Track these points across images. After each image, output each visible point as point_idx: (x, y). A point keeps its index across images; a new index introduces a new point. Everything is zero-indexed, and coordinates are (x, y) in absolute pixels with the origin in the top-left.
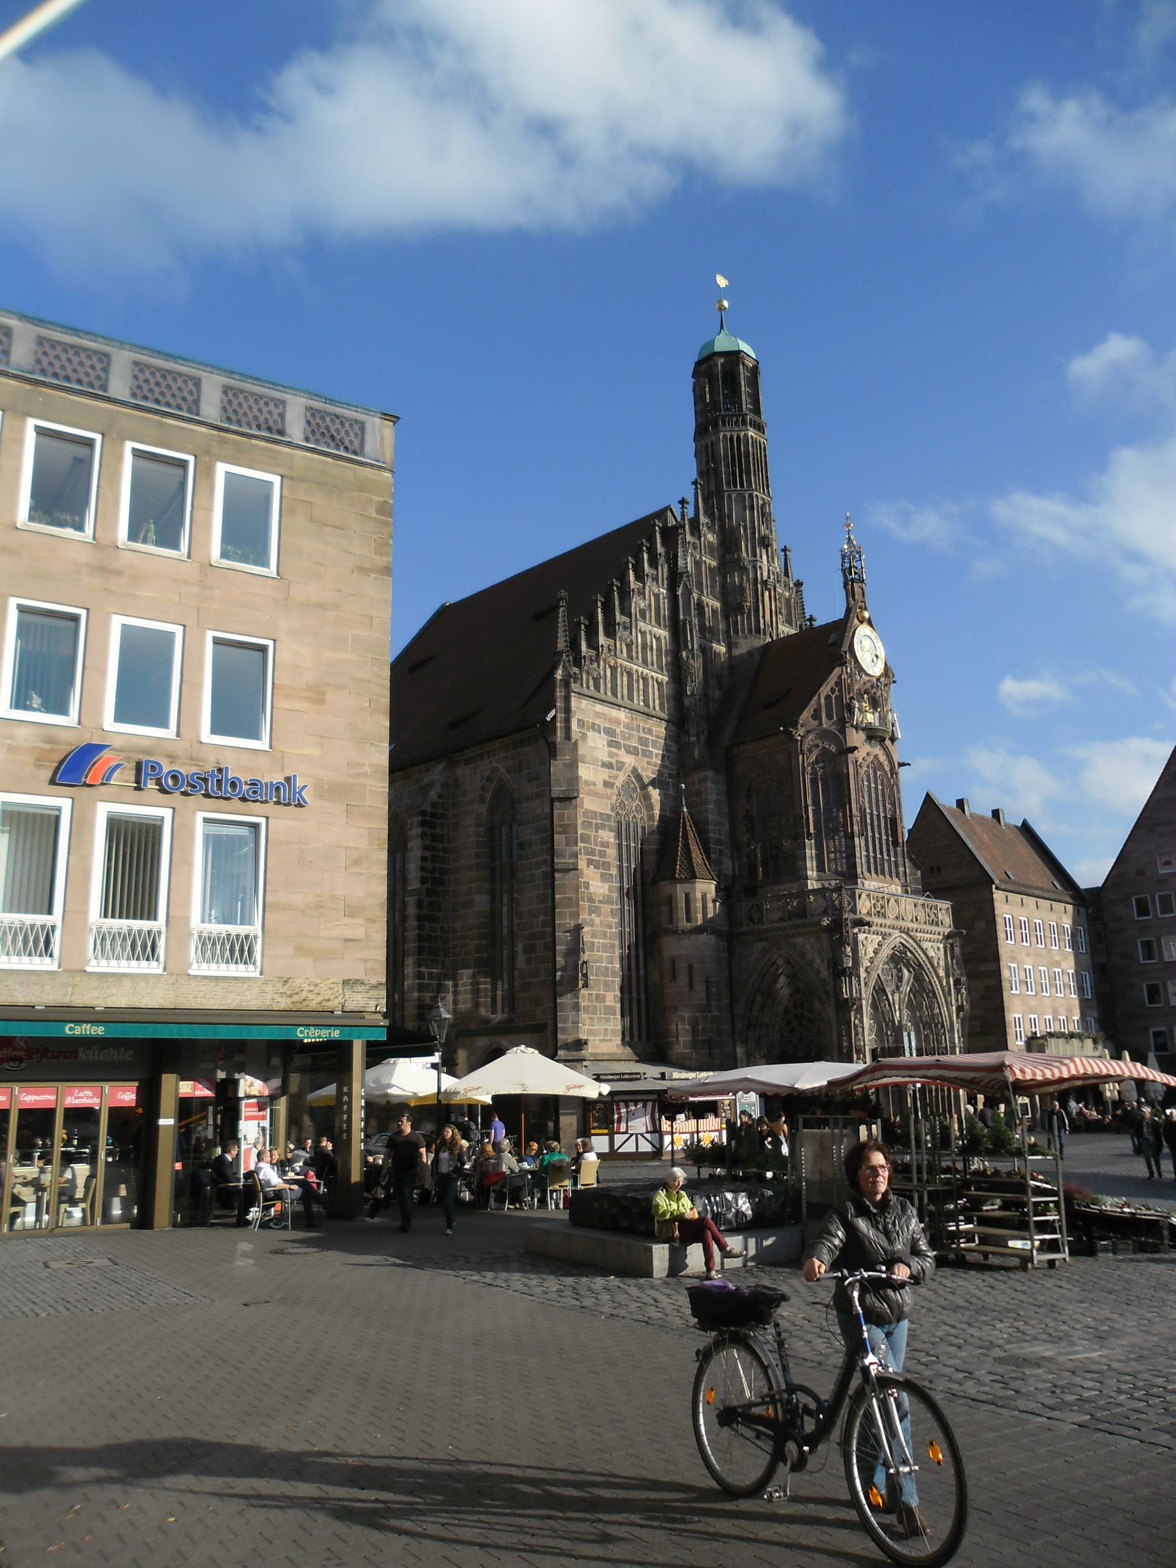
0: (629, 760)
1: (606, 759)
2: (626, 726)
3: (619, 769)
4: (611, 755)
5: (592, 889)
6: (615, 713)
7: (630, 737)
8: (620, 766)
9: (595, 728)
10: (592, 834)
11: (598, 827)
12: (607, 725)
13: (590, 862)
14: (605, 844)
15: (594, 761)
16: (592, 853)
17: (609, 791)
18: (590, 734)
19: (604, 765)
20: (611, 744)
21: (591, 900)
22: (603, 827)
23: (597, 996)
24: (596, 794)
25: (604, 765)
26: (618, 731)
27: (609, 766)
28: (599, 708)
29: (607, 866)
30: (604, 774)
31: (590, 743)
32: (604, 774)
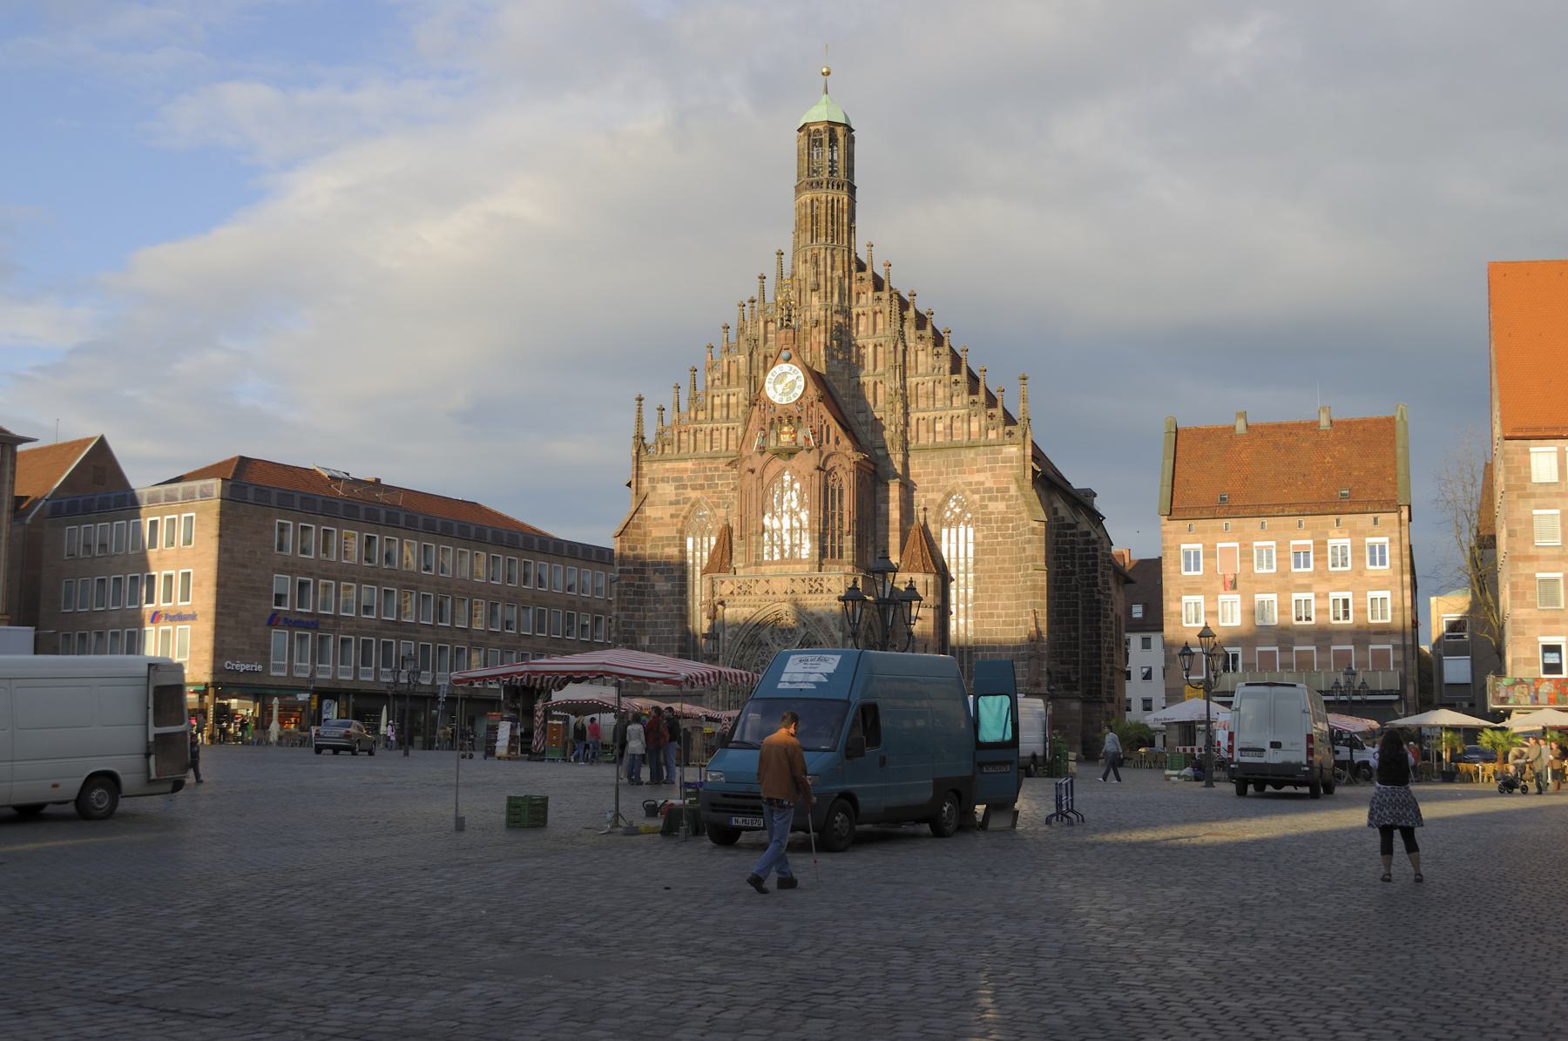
0: (693, 495)
2: (693, 471)
6: (682, 465)
8: (686, 501)
9: (663, 480)
13: (655, 571)
19: (671, 503)
21: (656, 594)
25: (671, 503)
27: (677, 503)
28: (668, 465)
30: (672, 509)
32: (672, 509)
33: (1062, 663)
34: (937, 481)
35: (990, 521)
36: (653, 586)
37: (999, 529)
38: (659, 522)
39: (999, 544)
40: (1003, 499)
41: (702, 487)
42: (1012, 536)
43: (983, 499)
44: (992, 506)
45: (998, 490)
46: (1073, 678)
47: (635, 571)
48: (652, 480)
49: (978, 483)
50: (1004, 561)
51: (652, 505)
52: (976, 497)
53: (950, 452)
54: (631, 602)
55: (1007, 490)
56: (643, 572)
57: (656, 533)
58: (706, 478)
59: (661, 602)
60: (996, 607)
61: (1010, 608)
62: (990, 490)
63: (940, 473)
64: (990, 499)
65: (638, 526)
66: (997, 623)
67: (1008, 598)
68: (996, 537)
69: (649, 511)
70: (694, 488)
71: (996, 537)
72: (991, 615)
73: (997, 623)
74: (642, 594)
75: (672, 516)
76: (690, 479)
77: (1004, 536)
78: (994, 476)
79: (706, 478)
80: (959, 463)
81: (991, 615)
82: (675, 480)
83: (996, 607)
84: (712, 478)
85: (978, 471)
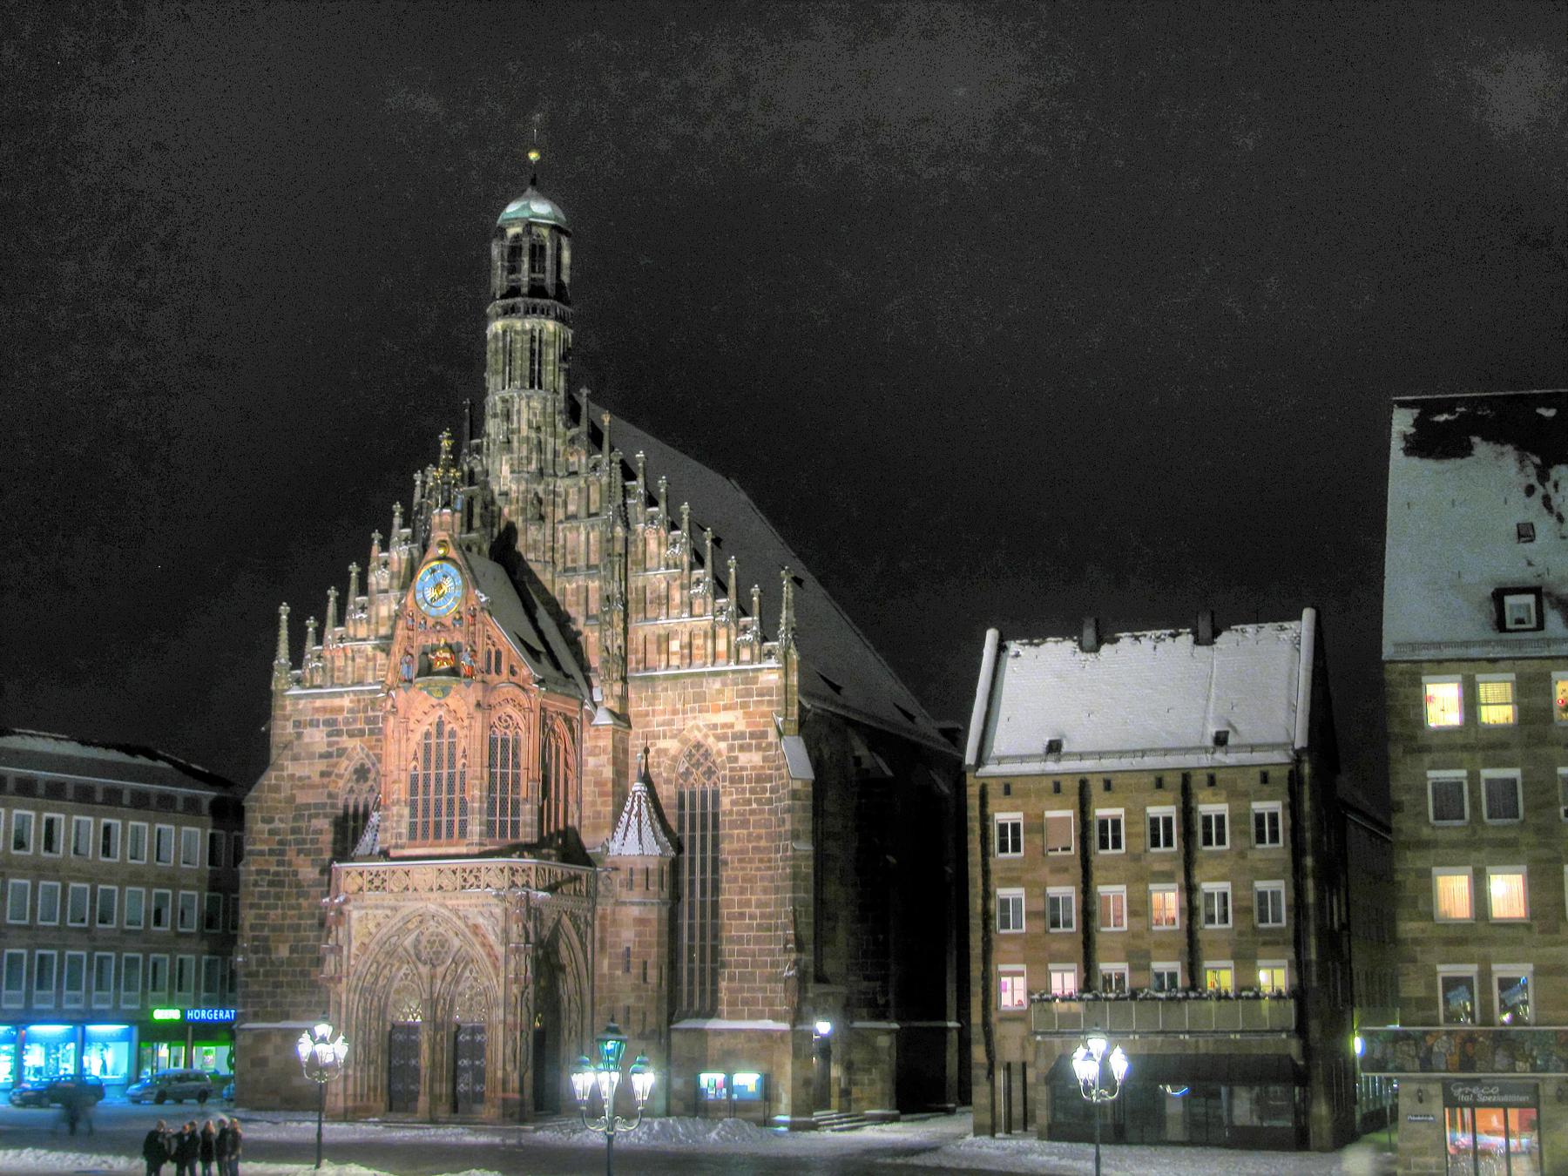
1: (324, 749)
2: (351, 711)
3: (339, 756)
4: (330, 744)
5: (300, 877)
6: (337, 702)
7: (355, 720)
9: (314, 724)
10: (303, 824)
11: (310, 817)
12: (328, 716)
13: (299, 852)
14: (320, 832)
15: (311, 756)
16: (304, 841)
17: (326, 780)
18: (307, 731)
19: (322, 756)
20: (329, 735)
21: (299, 885)
22: (317, 816)
23: (302, 972)
24: (312, 787)
25: (322, 756)
26: (340, 718)
27: (328, 755)
29: (320, 851)
30: (321, 765)
31: (307, 740)
33: (867, 978)
34: (670, 723)
35: (741, 779)
36: (296, 873)
37: (752, 791)
38: (303, 783)
39: (752, 812)
40: (759, 748)
41: (361, 733)
42: (770, 801)
43: (731, 748)
44: (745, 759)
45: (752, 735)
46: (881, 1001)
47: (272, 852)
48: (297, 724)
49: (724, 726)
50: (759, 837)
51: (295, 758)
52: (723, 745)
53: (689, 681)
54: (263, 896)
55: (764, 735)
56: (282, 853)
57: (302, 798)
58: (368, 721)
59: (306, 895)
60: (748, 903)
61: (767, 905)
62: (742, 735)
63: (675, 712)
64: (742, 748)
65: (276, 789)
66: (750, 928)
67: (765, 891)
68: (749, 802)
69: (291, 768)
70: (351, 735)
71: (749, 802)
72: (742, 916)
73: (750, 928)
74: (281, 884)
75: (323, 774)
76: (347, 722)
77: (758, 801)
78: (747, 715)
79: (368, 721)
80: (700, 698)
81: (742, 916)
82: (327, 723)
83: (748, 903)
84: (374, 721)
85: (726, 708)
